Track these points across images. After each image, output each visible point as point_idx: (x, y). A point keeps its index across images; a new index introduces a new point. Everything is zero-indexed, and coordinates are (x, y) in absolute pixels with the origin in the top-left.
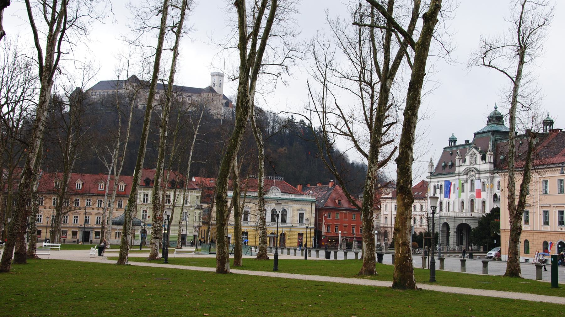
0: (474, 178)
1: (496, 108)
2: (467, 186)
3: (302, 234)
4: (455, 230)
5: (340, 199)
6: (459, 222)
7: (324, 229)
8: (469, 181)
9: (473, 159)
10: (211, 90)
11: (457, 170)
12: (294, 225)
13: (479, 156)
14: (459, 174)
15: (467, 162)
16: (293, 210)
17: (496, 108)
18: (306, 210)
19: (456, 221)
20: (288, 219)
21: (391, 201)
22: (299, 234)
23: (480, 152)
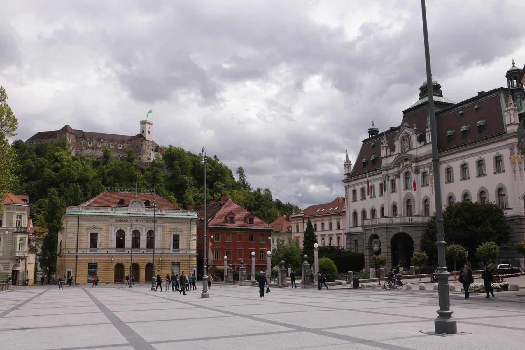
0: (410, 169)
2: (400, 183)
3: (178, 264)
4: (389, 244)
5: (231, 215)
6: (395, 232)
7: (211, 256)
8: (402, 175)
9: (406, 144)
10: (141, 137)
11: (384, 162)
12: (166, 252)
13: (414, 138)
15: (398, 150)
16: (164, 231)
18: (182, 231)
19: (389, 230)
20: (157, 244)
21: (302, 221)
22: (173, 264)
23: (416, 132)
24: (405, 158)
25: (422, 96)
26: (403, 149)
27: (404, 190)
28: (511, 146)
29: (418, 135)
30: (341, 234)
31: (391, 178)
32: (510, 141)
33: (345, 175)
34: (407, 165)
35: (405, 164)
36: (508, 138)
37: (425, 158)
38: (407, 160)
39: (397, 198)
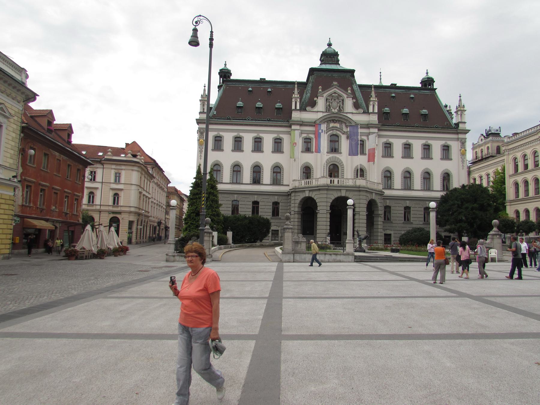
1: (330, 45)
11: (296, 115)
14: (302, 124)
17: (330, 45)
24: (336, 119)
25: (323, 61)
26: (328, 108)
27: (328, 152)
28: (463, 140)
29: (355, 101)
30: (97, 188)
31: (304, 135)
32: (461, 136)
33: (200, 113)
34: (336, 127)
35: (332, 125)
36: (461, 133)
37: (368, 126)
38: (334, 121)
39: (319, 161)
